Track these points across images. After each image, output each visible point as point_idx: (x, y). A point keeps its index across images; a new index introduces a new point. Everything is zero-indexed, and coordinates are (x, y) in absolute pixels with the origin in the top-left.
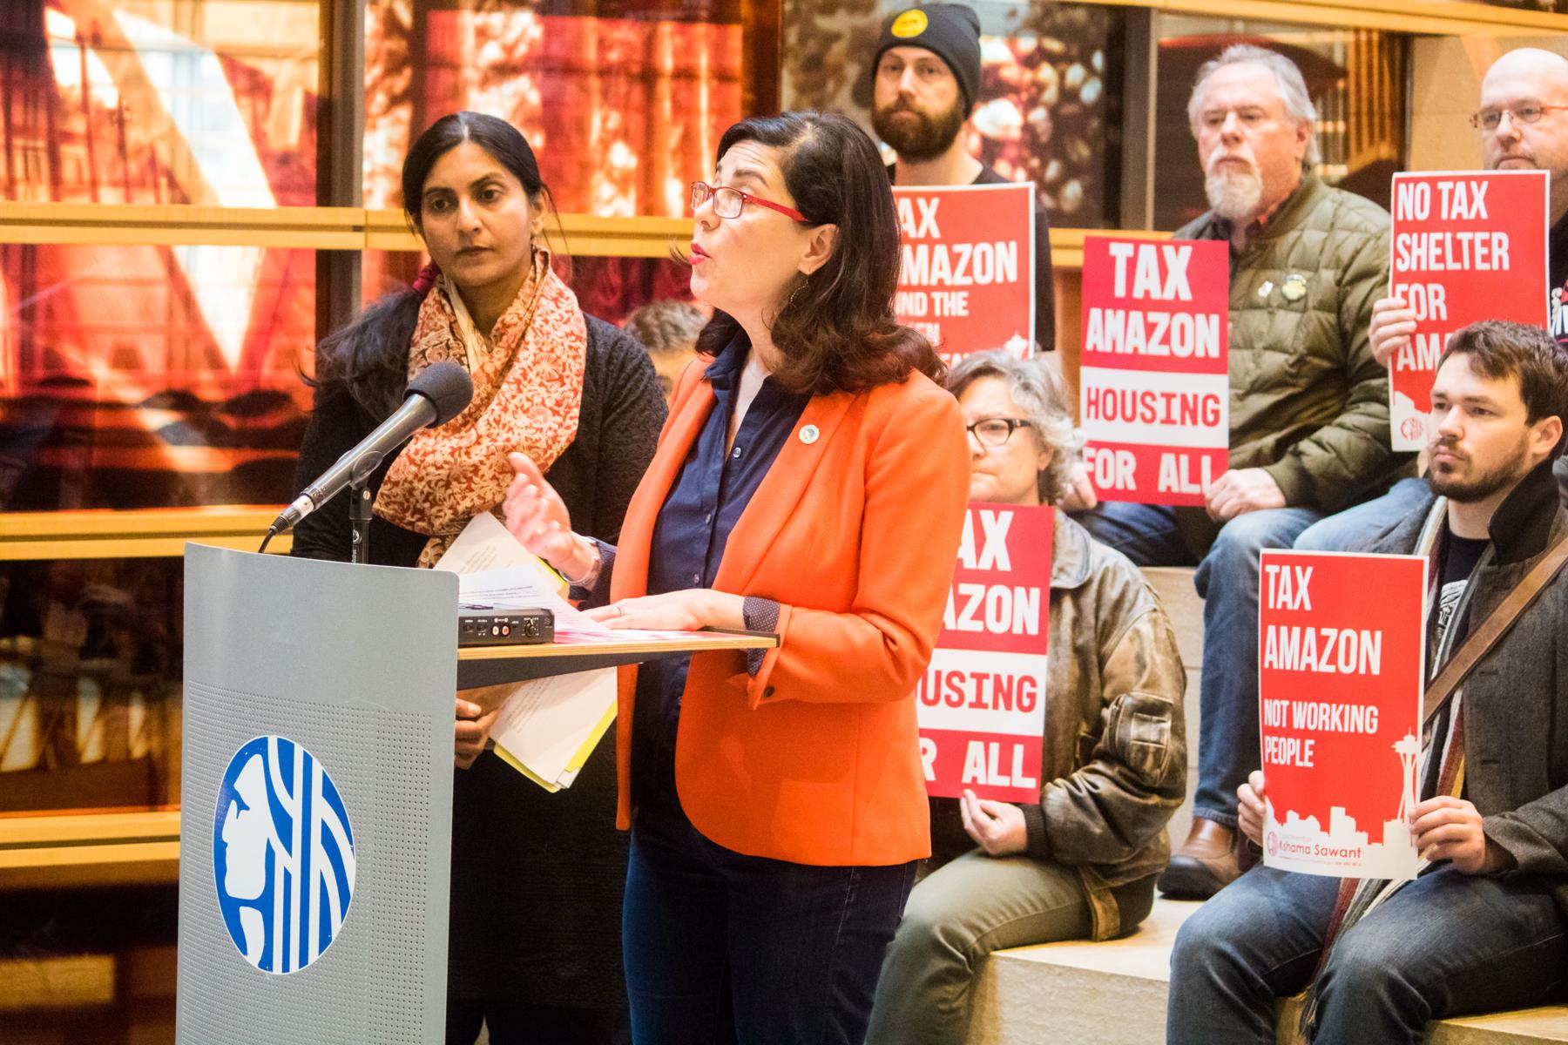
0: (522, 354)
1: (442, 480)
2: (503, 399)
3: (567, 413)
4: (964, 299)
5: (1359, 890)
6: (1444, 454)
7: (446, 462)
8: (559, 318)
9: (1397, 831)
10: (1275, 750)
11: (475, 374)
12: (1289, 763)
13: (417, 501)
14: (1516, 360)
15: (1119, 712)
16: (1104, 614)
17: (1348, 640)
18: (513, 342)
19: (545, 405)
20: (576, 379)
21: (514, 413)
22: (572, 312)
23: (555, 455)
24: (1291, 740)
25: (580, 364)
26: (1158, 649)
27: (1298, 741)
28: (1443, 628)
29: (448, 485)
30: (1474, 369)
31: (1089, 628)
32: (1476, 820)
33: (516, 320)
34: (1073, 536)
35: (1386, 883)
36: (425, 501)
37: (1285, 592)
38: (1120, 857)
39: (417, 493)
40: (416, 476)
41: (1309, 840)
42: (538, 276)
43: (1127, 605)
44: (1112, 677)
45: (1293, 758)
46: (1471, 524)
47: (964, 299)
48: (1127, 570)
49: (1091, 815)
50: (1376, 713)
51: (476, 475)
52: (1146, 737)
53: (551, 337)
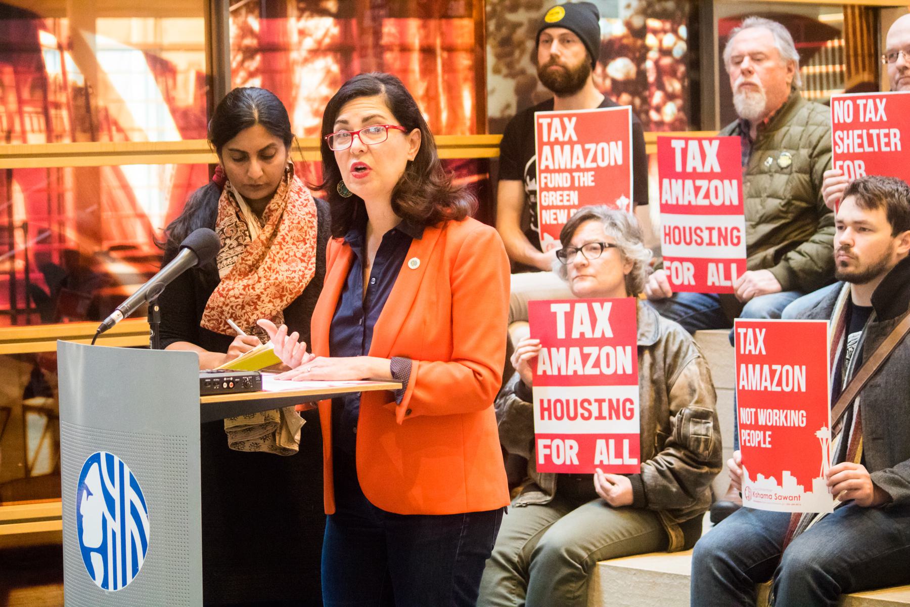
0: (282, 227)
1: (239, 305)
3: (309, 261)
4: (592, 176)
5: (802, 518)
6: (843, 256)
7: (241, 294)
8: (301, 204)
9: (819, 483)
10: (748, 438)
11: (255, 241)
12: (757, 445)
13: (226, 318)
14: (883, 197)
15: (682, 418)
16: (669, 360)
17: (787, 371)
18: (276, 221)
19: (296, 257)
20: (312, 240)
21: (278, 262)
22: (308, 200)
23: (304, 286)
24: (758, 432)
25: (315, 231)
26: (702, 380)
27: (762, 432)
28: (849, 360)
29: (243, 307)
30: (858, 204)
31: (660, 369)
32: (866, 476)
33: (277, 207)
34: (649, 314)
35: (816, 515)
37: (750, 344)
38: (688, 505)
39: (225, 313)
40: (224, 303)
41: (771, 491)
42: (289, 179)
43: (682, 355)
44: (676, 397)
45: (759, 442)
46: (863, 297)
47: (592, 176)
48: (681, 334)
49: (670, 482)
50: (805, 415)
51: (259, 300)
52: (699, 432)
53: (298, 215)
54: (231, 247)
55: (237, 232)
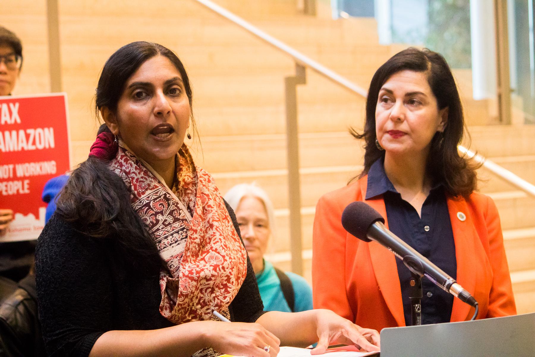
2: (221, 232)
7: (213, 276)
13: (193, 305)
29: (212, 292)
36: (197, 304)
39: (194, 299)
51: (229, 282)
54: (166, 223)
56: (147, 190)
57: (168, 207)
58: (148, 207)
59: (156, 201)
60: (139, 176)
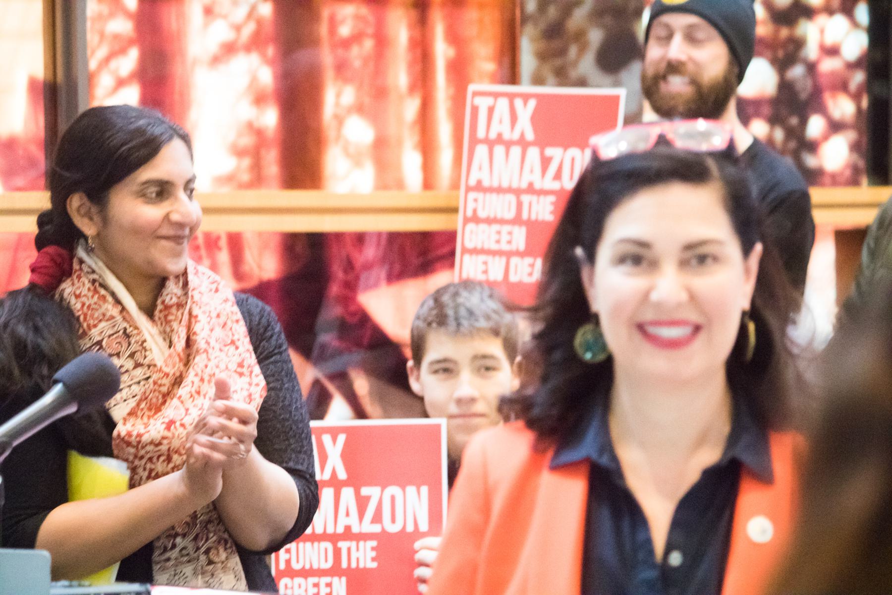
0: (197, 328)
40: (136, 456)
55: (129, 344)
56: (100, 321)
57: (128, 347)
58: (98, 347)
59: (111, 338)
60: (92, 301)
